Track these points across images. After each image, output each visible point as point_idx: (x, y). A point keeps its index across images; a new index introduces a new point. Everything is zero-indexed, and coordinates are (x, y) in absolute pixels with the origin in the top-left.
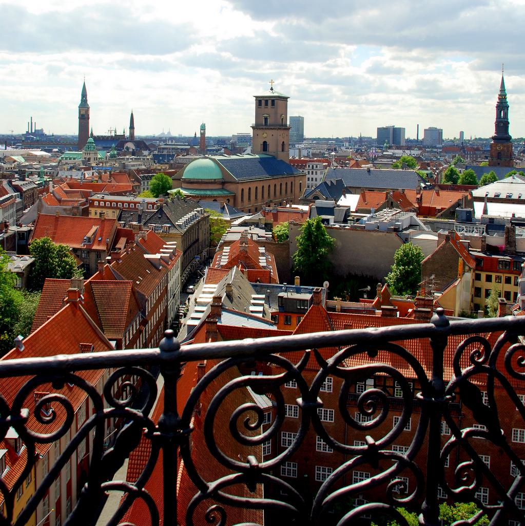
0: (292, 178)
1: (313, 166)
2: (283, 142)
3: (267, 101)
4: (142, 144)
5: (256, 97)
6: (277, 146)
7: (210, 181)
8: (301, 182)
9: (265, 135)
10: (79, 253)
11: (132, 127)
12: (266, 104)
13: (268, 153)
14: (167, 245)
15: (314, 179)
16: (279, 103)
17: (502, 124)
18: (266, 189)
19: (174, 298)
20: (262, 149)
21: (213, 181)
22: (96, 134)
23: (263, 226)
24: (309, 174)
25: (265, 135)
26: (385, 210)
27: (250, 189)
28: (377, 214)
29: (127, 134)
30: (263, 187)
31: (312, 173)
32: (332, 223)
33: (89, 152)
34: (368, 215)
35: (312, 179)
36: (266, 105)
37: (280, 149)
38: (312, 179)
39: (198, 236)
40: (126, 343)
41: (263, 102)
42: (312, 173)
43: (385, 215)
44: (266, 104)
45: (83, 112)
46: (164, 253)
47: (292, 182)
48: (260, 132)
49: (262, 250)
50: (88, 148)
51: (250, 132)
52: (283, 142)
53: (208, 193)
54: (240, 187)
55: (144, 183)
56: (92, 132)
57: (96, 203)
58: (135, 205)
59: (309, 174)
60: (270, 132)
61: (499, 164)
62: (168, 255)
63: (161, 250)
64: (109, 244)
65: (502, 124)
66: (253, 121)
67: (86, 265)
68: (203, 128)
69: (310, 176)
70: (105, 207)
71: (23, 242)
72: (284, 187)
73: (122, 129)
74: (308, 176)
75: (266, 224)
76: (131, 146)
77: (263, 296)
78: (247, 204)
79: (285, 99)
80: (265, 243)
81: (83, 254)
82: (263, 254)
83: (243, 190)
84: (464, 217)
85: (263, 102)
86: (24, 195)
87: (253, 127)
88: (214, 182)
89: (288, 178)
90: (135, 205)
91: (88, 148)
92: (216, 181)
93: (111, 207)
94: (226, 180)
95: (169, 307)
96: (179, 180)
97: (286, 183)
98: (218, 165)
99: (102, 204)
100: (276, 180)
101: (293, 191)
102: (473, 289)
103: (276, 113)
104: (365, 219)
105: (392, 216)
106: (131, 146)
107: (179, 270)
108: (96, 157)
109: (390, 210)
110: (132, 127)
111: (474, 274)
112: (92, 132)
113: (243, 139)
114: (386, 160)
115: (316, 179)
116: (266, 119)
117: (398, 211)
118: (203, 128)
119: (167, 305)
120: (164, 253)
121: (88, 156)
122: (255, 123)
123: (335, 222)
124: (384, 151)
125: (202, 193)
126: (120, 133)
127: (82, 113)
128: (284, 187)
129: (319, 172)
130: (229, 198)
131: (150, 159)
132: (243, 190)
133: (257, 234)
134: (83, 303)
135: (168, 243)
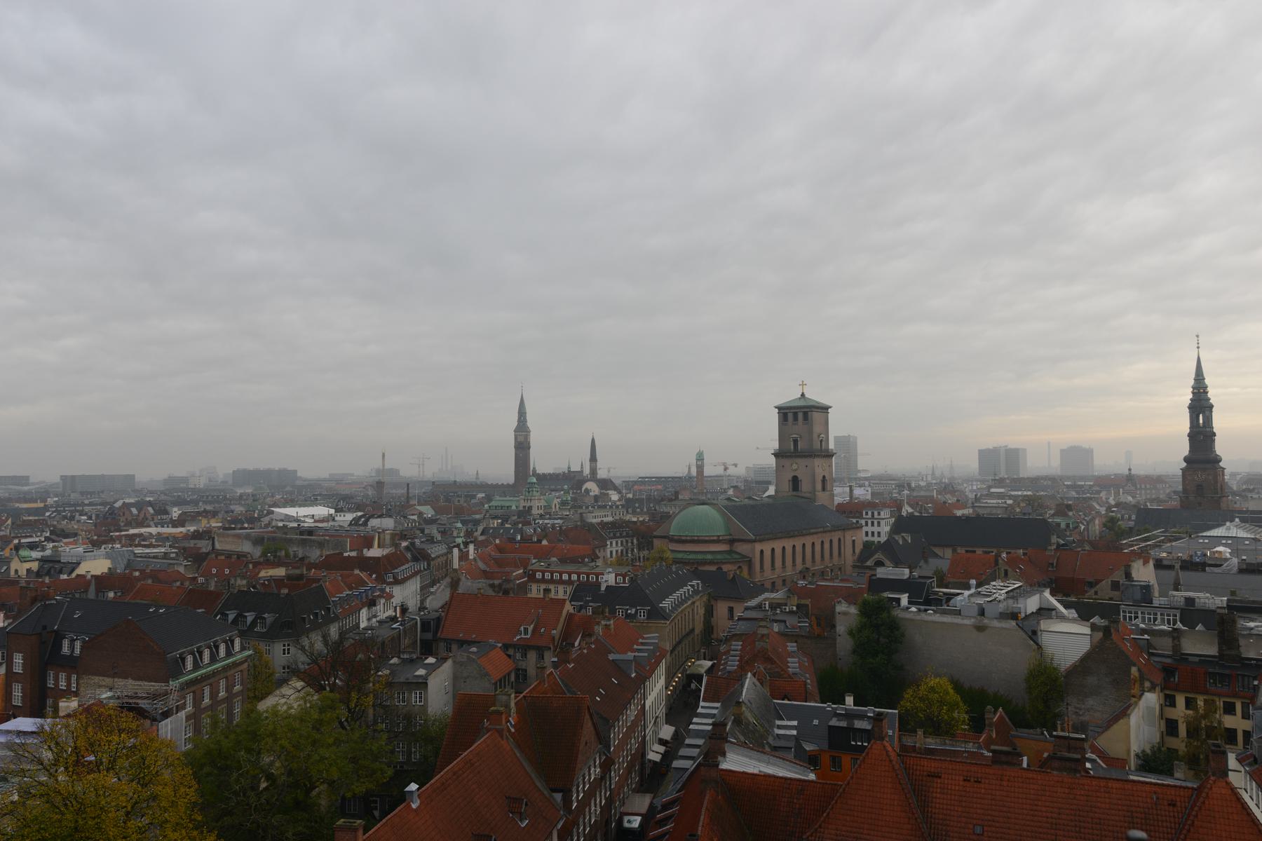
0: (840, 532)
1: (873, 513)
2: (824, 477)
3: (795, 415)
4: (605, 484)
5: (780, 408)
6: (814, 482)
7: (712, 538)
8: (854, 538)
9: (795, 466)
10: (511, 652)
11: (593, 458)
12: (796, 418)
13: (800, 494)
14: (644, 638)
15: (876, 534)
16: (816, 416)
17: (1202, 436)
18: (799, 549)
19: (655, 722)
20: (791, 490)
21: (715, 538)
22: (541, 470)
23: (795, 608)
24: (867, 525)
25: (795, 466)
26: (994, 583)
27: (773, 550)
28: (979, 590)
29: (587, 471)
30: (794, 546)
31: (873, 523)
33: (529, 498)
34: (967, 593)
35: (873, 533)
36: (795, 421)
37: (819, 486)
38: (873, 533)
40: (578, 796)
41: (790, 416)
42: (873, 523)
43: (995, 591)
44: (796, 418)
45: (521, 439)
46: (639, 651)
47: (840, 540)
48: (787, 462)
49: (792, 647)
50: (529, 492)
52: (824, 477)
54: (758, 547)
55: (611, 543)
56: (534, 468)
57: (539, 576)
58: (597, 578)
59: (867, 525)
60: (802, 462)
61: (1200, 504)
62: (646, 654)
63: (635, 647)
64: (557, 638)
65: (1202, 436)
66: (776, 446)
67: (522, 670)
68: (700, 457)
69: (869, 529)
70: (552, 581)
71: (429, 636)
72: (827, 546)
73: (577, 461)
74: (865, 529)
75: (798, 606)
76: (592, 487)
77: (795, 723)
79: (825, 409)
80: (797, 636)
81: (517, 654)
82: (791, 655)
83: (762, 552)
84: (1138, 596)
85: (790, 416)
86: (432, 563)
87: (776, 455)
89: (833, 533)
90: (597, 578)
91: (529, 492)
92: (721, 538)
93: (561, 582)
94: (737, 537)
95: (648, 738)
96: (664, 537)
97: (831, 541)
98: (723, 514)
99: (548, 576)
100: (815, 536)
101: (843, 555)
102: (1163, 723)
103: (811, 432)
104: (959, 598)
105: (1006, 593)
106: (592, 487)
107: (663, 678)
108: (539, 505)
109: (1002, 584)
110: (593, 458)
111: (1162, 695)
112: (534, 468)
114: (995, 501)
115: (879, 533)
116: (795, 441)
117: (1016, 586)
118: (700, 457)
119: (645, 733)
120: (639, 651)
121: (528, 504)
123: (910, 603)
125: (700, 557)
126: (575, 468)
127: (519, 440)
128: (827, 546)
129: (883, 523)
130: (741, 565)
131: (620, 507)
132: (762, 552)
133: (785, 622)
134: (513, 730)
135: (645, 636)
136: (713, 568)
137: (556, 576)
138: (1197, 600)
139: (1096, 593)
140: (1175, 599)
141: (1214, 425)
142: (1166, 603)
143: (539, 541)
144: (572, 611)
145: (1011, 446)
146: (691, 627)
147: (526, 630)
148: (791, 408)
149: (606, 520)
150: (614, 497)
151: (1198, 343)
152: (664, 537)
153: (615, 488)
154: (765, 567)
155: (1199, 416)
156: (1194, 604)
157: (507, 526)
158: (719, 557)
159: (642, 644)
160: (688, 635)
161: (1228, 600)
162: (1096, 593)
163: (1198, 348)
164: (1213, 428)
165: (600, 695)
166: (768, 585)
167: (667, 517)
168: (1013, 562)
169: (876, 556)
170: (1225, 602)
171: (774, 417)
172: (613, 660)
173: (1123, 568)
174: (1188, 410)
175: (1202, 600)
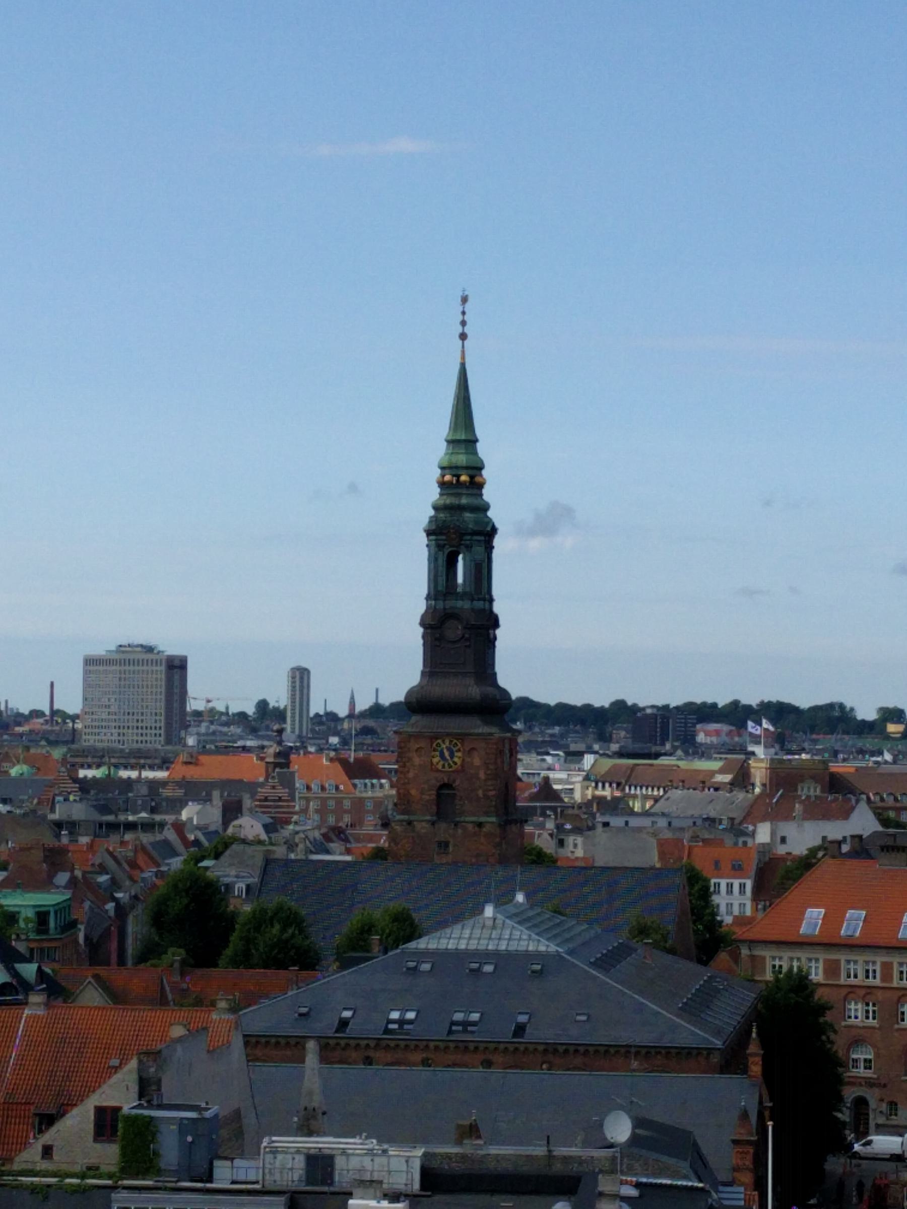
61: (444, 845)
138: (340, 1162)
139: (47, 1151)
140: (278, 1164)
141: (495, 592)
142: (252, 1178)
151: (463, 323)
155: (456, 561)
156: (331, 1175)
161: (425, 1155)
162: (47, 1151)
163: (463, 336)
164: (491, 600)
170: (417, 1165)
173: (133, 1064)
174: (423, 539)
175: (354, 1162)
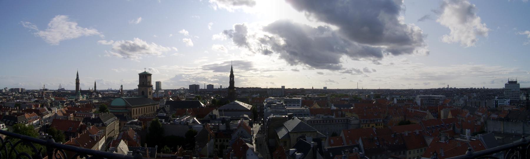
3: (143, 76)
4: (98, 92)
22: (82, 89)
25: (143, 89)
32: (163, 121)
37: (149, 94)
39: (114, 128)
51: (137, 87)
53: (121, 111)
57: (77, 115)
66: (138, 84)
68: (122, 86)
69: (161, 104)
78: (135, 115)
83: (134, 110)
88: (123, 107)
93: (82, 117)
98: (124, 100)
106: (95, 93)
113: (135, 90)
116: (143, 83)
118: (122, 86)
122: (138, 84)
124: (191, 94)
125: (118, 111)
126: (91, 89)
132: (134, 110)
133: (135, 127)
136: (121, 114)
137: (81, 115)
143: (78, 107)
144: (82, 124)
145: (196, 84)
146: (114, 128)
147: (71, 128)
148: (142, 74)
149: (96, 102)
150: (100, 96)
152: (109, 106)
153: (101, 94)
154: (137, 113)
157: (72, 103)
158: (123, 111)
159: (99, 132)
160: (113, 130)
165: (86, 145)
166: (135, 118)
167: (111, 101)
168: (189, 111)
169: (161, 111)
171: (138, 76)
172: (90, 136)
